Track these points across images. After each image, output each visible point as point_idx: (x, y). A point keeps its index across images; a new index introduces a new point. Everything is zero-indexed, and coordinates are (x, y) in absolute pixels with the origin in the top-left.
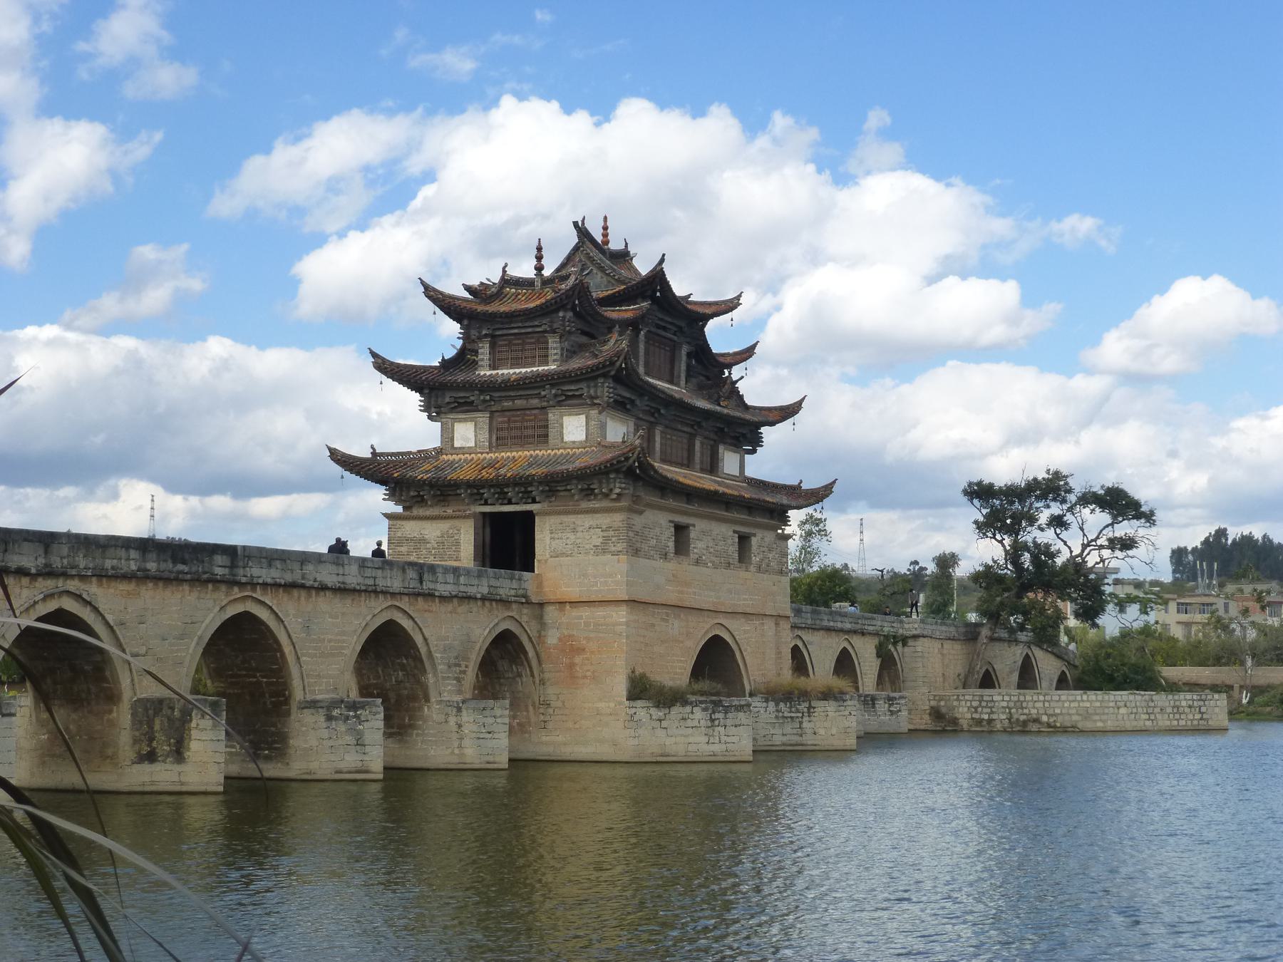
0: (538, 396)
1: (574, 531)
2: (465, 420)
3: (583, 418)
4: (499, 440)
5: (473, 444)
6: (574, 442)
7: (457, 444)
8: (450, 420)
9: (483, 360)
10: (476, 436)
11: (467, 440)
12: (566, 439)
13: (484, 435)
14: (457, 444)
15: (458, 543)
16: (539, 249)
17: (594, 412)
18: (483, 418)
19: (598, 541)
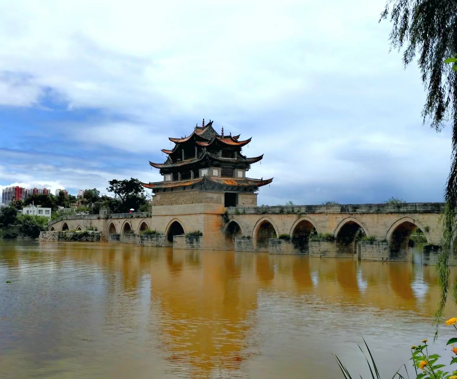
0: (228, 165)
1: (247, 199)
2: (216, 169)
3: (242, 172)
4: (223, 175)
5: (217, 175)
6: (240, 177)
7: (214, 175)
8: (212, 169)
9: (220, 155)
10: (218, 173)
11: (216, 174)
12: (238, 176)
13: (220, 174)
14: (214, 175)
15: (221, 199)
16: (223, 129)
17: (244, 171)
18: (220, 169)
19: (251, 201)
